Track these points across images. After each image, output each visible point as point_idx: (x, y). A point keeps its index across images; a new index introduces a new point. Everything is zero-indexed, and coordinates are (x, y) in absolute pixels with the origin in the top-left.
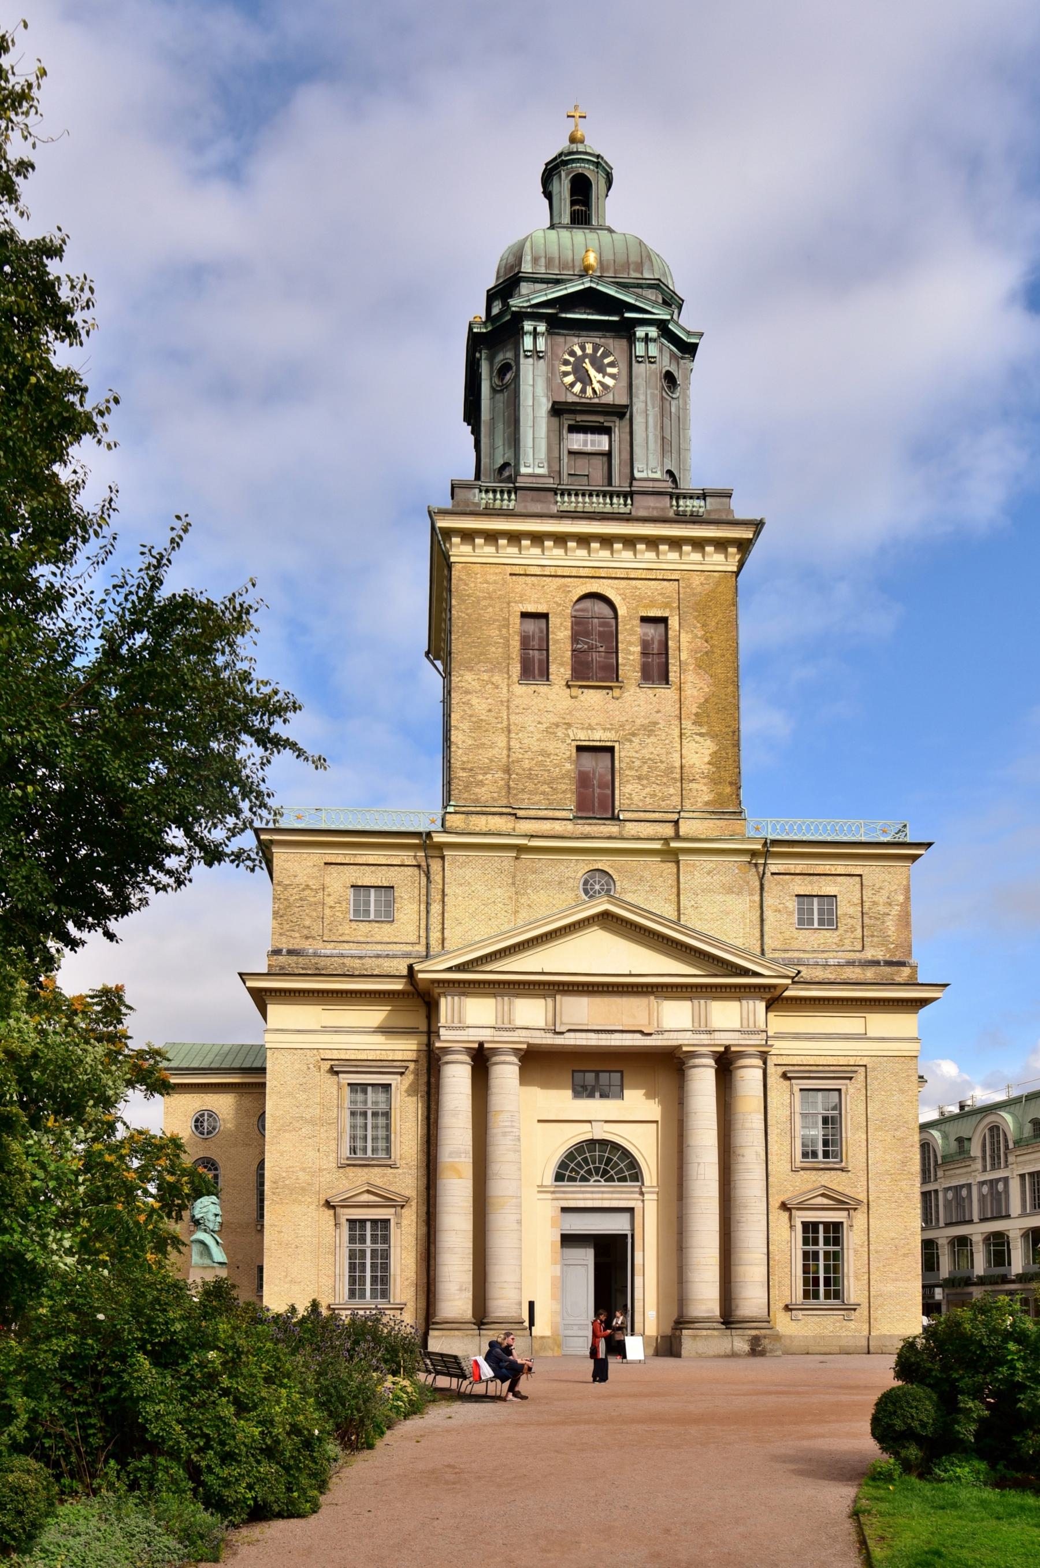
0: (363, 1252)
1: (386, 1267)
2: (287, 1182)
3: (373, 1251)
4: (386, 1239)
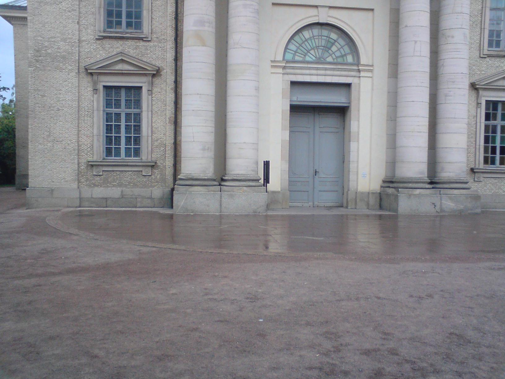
0: (118, 115)
1: (138, 128)
2: (49, 51)
3: (128, 115)
4: (138, 103)
